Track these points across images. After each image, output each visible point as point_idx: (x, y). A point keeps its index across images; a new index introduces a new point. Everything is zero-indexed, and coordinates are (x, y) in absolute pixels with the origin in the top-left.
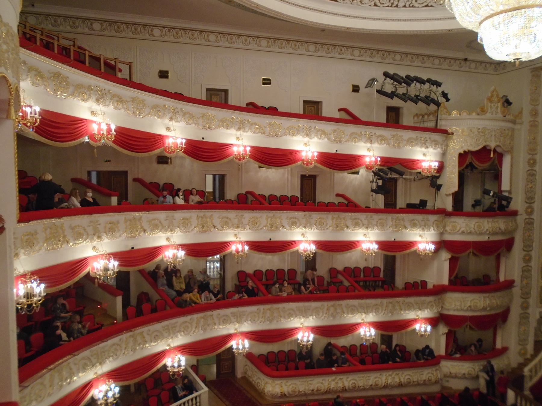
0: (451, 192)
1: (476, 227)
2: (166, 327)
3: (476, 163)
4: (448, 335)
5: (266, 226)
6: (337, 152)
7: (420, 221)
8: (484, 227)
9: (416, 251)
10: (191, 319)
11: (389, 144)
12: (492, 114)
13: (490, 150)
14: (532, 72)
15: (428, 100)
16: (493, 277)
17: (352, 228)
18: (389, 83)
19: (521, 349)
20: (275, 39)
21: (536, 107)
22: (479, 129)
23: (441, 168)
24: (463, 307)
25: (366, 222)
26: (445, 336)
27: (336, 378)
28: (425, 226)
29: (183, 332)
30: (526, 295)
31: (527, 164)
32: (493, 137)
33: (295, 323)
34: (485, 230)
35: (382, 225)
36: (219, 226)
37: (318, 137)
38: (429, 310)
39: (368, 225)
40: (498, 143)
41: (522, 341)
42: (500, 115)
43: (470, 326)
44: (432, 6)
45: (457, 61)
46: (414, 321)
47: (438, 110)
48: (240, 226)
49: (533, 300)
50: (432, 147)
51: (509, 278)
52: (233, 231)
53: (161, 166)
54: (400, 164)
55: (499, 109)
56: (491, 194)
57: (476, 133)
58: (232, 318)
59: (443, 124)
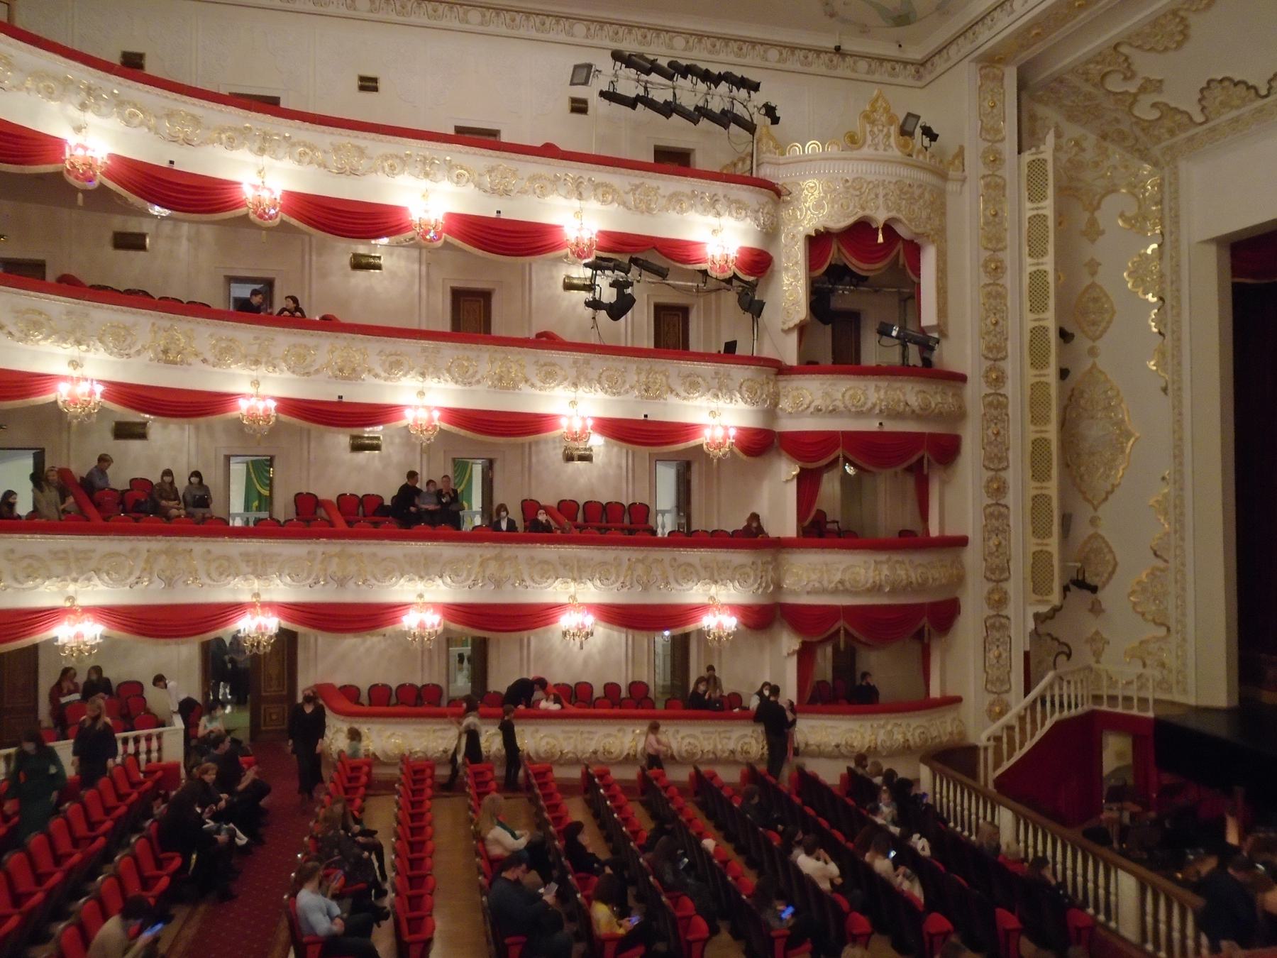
0: (791, 324)
1: (847, 397)
2: (62, 555)
3: (855, 265)
4: (805, 656)
6: (503, 216)
7: (709, 379)
8: (867, 399)
9: (701, 445)
10: (132, 550)
11: (624, 204)
13: (877, 229)
15: (725, 119)
17: (539, 384)
18: (628, 78)
19: (992, 704)
21: (998, 145)
23: (758, 263)
24: (825, 583)
26: (793, 661)
28: (720, 389)
29: (108, 574)
30: (997, 573)
32: (881, 200)
34: (869, 405)
35: (613, 385)
37: (452, 181)
38: (737, 584)
39: (578, 377)
40: (893, 214)
41: (996, 685)
42: (896, 152)
43: (846, 630)
45: (822, 56)
46: (703, 608)
48: (264, 360)
49: (1016, 586)
50: (730, 214)
51: (950, 532)
52: (246, 372)
53: (121, 253)
54: (655, 248)
55: (892, 140)
56: (894, 333)
58: (243, 567)
59: (766, 172)
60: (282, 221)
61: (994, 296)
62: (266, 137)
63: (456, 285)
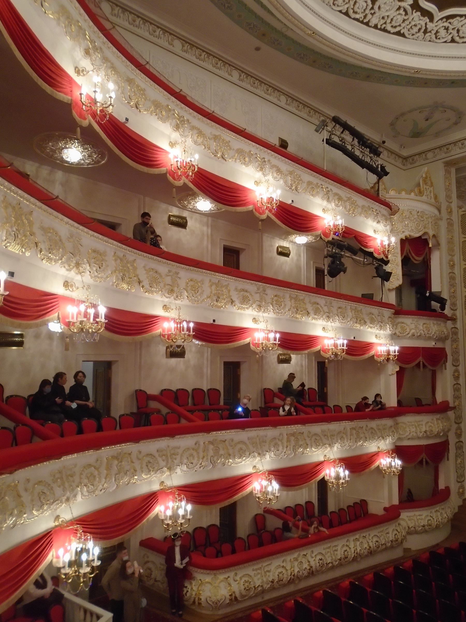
0: (394, 287)
1: (425, 329)
5: (209, 297)
11: (345, 208)
12: (428, 198)
14: (445, 166)
16: (426, 399)
19: (459, 489)
20: (193, 45)
22: (418, 212)
25: (326, 309)
27: (299, 555)
31: (448, 265)
33: (243, 466)
34: (433, 333)
36: (146, 283)
44: (403, 35)
47: (378, 182)
57: (416, 216)
58: (160, 460)
60: (185, 184)
61: (452, 278)
62: (181, 118)
63: (227, 244)
